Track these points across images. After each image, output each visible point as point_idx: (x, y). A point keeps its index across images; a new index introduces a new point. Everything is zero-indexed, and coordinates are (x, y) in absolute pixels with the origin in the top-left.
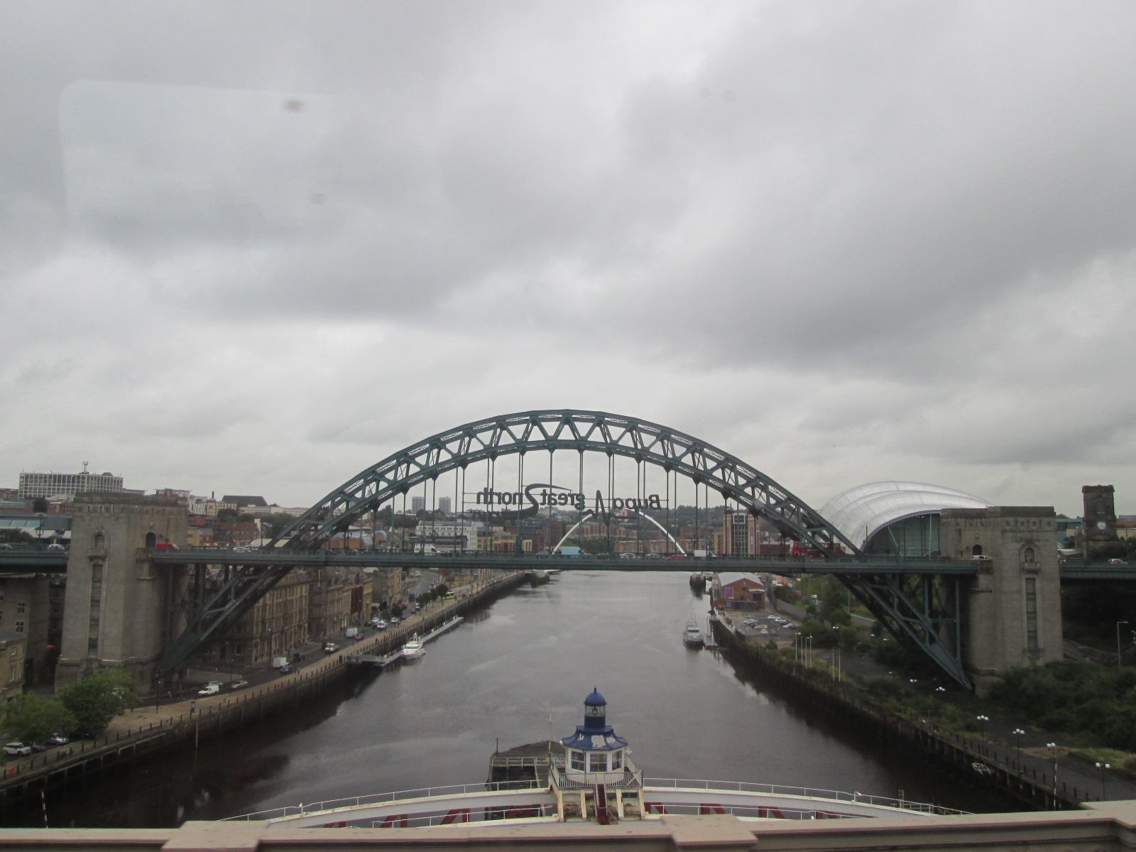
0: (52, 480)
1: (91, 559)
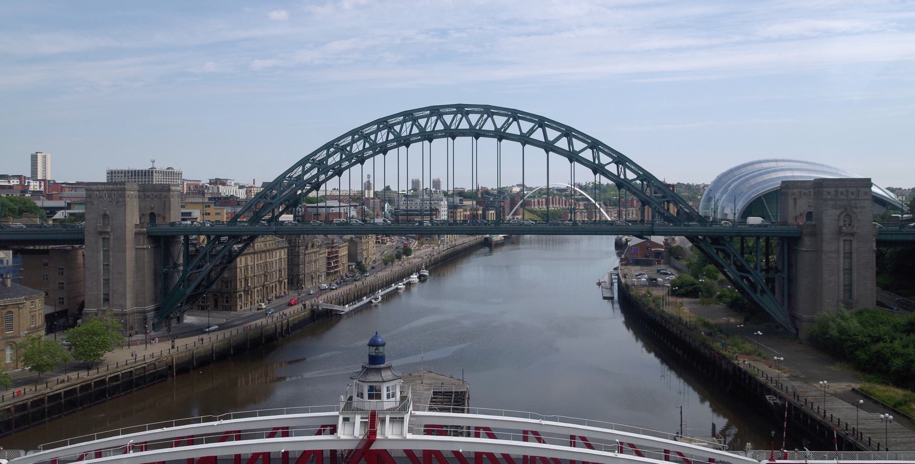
1: (101, 233)
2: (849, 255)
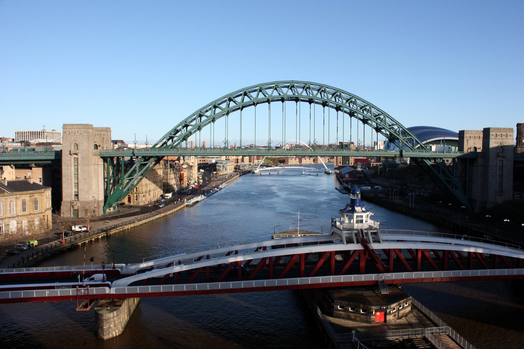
0: (30, 134)
2: (501, 168)
